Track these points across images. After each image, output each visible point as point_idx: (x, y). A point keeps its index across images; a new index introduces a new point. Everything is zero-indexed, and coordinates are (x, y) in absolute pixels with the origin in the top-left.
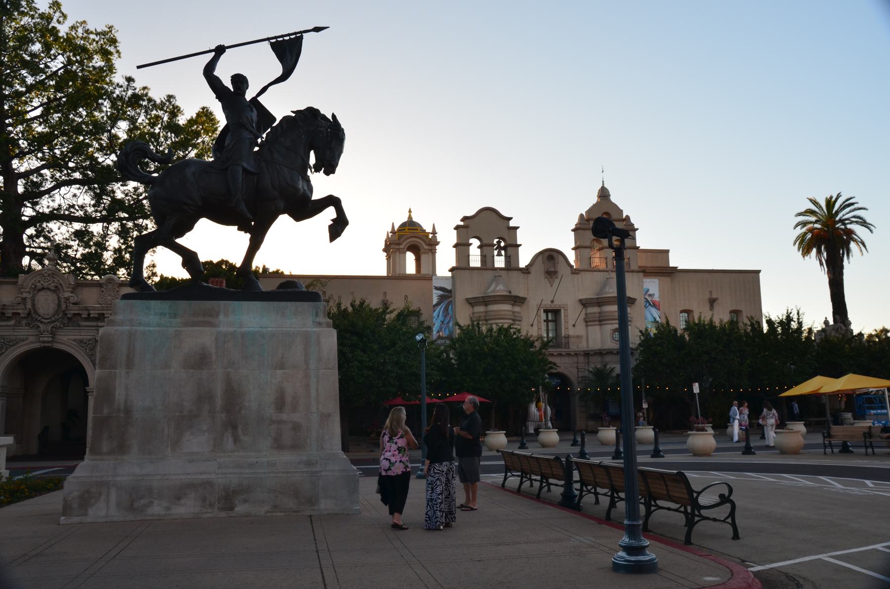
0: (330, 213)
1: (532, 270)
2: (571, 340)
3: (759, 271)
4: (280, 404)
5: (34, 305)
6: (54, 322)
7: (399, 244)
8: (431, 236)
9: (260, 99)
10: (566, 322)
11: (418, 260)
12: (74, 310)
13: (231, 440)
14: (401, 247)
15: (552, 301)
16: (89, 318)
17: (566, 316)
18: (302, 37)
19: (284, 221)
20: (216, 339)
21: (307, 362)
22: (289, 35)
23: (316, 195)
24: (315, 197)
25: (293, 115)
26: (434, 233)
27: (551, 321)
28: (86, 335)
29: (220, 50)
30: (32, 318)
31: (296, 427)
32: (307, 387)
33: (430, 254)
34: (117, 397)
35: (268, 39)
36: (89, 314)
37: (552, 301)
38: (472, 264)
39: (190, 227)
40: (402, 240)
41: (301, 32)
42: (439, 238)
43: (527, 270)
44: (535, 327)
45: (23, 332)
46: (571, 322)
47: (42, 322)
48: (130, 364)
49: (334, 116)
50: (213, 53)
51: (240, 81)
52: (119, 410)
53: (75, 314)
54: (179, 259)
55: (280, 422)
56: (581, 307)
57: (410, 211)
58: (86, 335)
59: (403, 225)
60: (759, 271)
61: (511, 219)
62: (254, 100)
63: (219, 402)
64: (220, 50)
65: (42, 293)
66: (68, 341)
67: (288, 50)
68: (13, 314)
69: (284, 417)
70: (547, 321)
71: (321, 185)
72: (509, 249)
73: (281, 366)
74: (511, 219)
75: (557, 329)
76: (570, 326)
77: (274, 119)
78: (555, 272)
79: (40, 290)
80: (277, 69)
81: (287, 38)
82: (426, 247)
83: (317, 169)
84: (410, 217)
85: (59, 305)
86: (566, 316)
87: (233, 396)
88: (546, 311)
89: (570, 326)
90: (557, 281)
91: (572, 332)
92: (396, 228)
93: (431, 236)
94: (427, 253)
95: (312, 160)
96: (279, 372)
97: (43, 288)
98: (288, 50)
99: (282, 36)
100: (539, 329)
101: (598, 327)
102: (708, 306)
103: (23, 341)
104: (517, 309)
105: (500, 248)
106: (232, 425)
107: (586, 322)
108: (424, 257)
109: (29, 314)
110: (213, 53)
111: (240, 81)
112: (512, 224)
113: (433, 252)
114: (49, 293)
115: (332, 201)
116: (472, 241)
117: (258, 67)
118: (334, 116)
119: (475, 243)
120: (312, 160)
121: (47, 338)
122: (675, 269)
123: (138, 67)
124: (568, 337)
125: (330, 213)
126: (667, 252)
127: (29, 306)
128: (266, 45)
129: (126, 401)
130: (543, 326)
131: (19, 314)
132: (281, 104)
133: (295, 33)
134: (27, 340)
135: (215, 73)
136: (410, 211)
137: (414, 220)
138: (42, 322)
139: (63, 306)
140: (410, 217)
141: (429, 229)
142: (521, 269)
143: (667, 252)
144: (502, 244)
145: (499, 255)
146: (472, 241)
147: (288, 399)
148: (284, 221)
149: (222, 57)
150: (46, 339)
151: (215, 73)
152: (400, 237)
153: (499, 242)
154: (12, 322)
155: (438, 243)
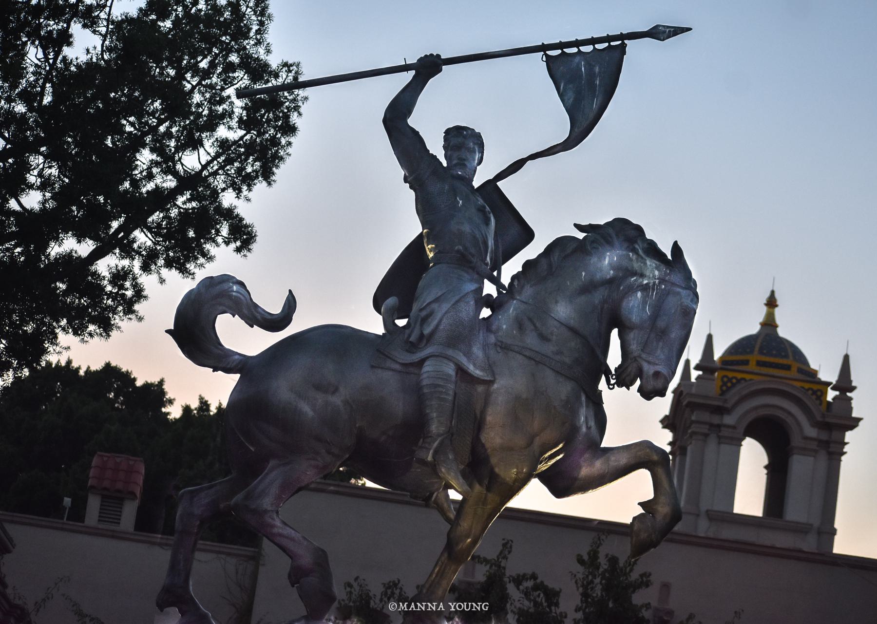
7: (721, 411)
8: (831, 395)
9: (503, 185)
11: (777, 474)
14: (729, 420)
18: (622, 49)
22: (593, 41)
25: (581, 235)
26: (845, 384)
29: (428, 67)
33: (822, 461)
35: (543, 48)
40: (732, 397)
41: (622, 37)
49: (676, 249)
50: (410, 75)
51: (463, 141)
57: (772, 303)
59: (742, 347)
62: (491, 185)
64: (428, 67)
67: (586, 78)
77: (528, 235)
80: (562, 129)
82: (811, 432)
83: (623, 379)
84: (769, 324)
92: (717, 354)
93: (831, 395)
94: (805, 451)
95: (614, 359)
98: (586, 78)
99: (577, 43)
108: (800, 466)
110: (410, 75)
111: (463, 141)
113: (834, 451)
118: (676, 249)
120: (614, 359)
132: (553, 206)
133: (608, 39)
135: (412, 121)
136: (772, 303)
137: (782, 332)
140: (769, 324)
141: (829, 374)
151: (412, 121)
152: (727, 386)
155: (854, 423)
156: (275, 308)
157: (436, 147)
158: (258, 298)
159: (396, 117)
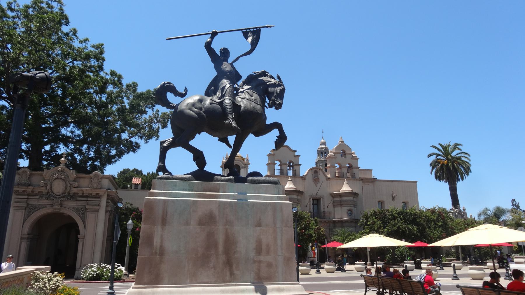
0: (275, 133)
1: (307, 178)
2: (326, 215)
3: (417, 182)
4: (259, 250)
5: (51, 188)
6: (62, 197)
10: (324, 205)
12: (74, 191)
13: (228, 273)
15: (317, 194)
16: (83, 196)
17: (323, 202)
18: (260, 31)
19: (251, 136)
20: (219, 206)
21: (275, 223)
22: (253, 28)
23: (268, 122)
24: (268, 122)
27: (316, 204)
28: (80, 204)
29: (214, 34)
30: (49, 195)
31: (269, 265)
32: (275, 238)
34: (155, 244)
35: (242, 30)
36: (83, 193)
37: (317, 194)
38: (276, 174)
39: (193, 138)
41: (259, 28)
42: (250, 161)
43: (304, 177)
44: (308, 208)
45: (44, 202)
46: (326, 205)
47: (55, 197)
48: (164, 221)
50: (210, 35)
51: (225, 52)
52: (156, 253)
53: (74, 193)
54: (191, 155)
55: (260, 262)
56: (331, 198)
58: (80, 204)
60: (417, 182)
61: (296, 151)
63: (221, 248)
64: (214, 34)
65: (57, 180)
66: (69, 209)
68: (39, 192)
69: (262, 258)
70: (313, 204)
71: (272, 115)
72: (295, 167)
73: (259, 225)
74: (296, 151)
75: (319, 209)
76: (326, 207)
77: (240, 77)
78: (318, 180)
79: (56, 179)
81: (252, 30)
83: (270, 106)
85: (66, 188)
86: (323, 202)
87: (230, 243)
88: (313, 200)
89: (326, 207)
90: (319, 184)
91: (326, 210)
96: (258, 228)
97: (58, 178)
100: (310, 208)
101: (340, 208)
102: (391, 198)
103: (43, 208)
104: (299, 198)
105: (290, 166)
106: (229, 263)
107: (334, 205)
109: (48, 193)
111: (225, 52)
112: (296, 154)
114: (61, 180)
115: (277, 125)
116: (276, 162)
117: (237, 45)
119: (278, 163)
121: (57, 206)
122: (375, 180)
123: (167, 39)
124: (324, 213)
125: (275, 133)
126: (371, 170)
127: (48, 187)
128: (240, 33)
129: (161, 246)
130: (312, 206)
131: (42, 192)
133: (257, 28)
134: (46, 208)
138: (55, 197)
139: (68, 188)
142: (301, 177)
143: (371, 170)
144: (291, 164)
145: (290, 170)
146: (276, 162)
147: (264, 247)
148: (251, 136)
149: (216, 38)
150: (57, 207)
153: (290, 163)
154: (37, 197)
156: (182, 91)
157: (218, 53)
158: (177, 88)
159: (208, 46)
